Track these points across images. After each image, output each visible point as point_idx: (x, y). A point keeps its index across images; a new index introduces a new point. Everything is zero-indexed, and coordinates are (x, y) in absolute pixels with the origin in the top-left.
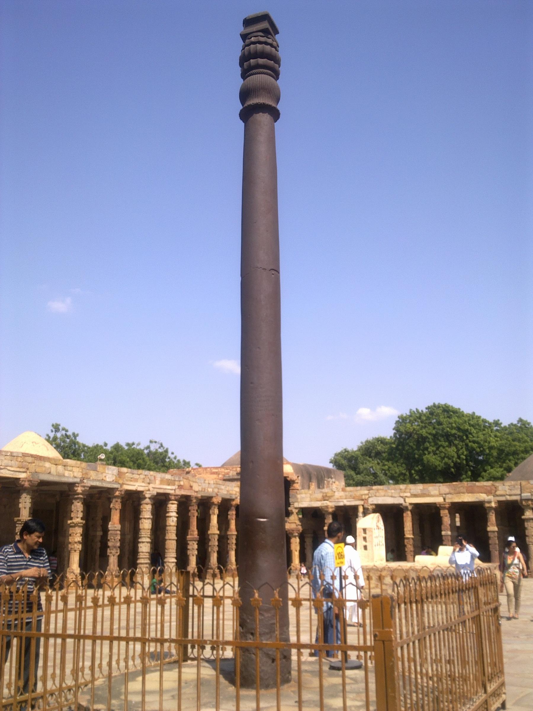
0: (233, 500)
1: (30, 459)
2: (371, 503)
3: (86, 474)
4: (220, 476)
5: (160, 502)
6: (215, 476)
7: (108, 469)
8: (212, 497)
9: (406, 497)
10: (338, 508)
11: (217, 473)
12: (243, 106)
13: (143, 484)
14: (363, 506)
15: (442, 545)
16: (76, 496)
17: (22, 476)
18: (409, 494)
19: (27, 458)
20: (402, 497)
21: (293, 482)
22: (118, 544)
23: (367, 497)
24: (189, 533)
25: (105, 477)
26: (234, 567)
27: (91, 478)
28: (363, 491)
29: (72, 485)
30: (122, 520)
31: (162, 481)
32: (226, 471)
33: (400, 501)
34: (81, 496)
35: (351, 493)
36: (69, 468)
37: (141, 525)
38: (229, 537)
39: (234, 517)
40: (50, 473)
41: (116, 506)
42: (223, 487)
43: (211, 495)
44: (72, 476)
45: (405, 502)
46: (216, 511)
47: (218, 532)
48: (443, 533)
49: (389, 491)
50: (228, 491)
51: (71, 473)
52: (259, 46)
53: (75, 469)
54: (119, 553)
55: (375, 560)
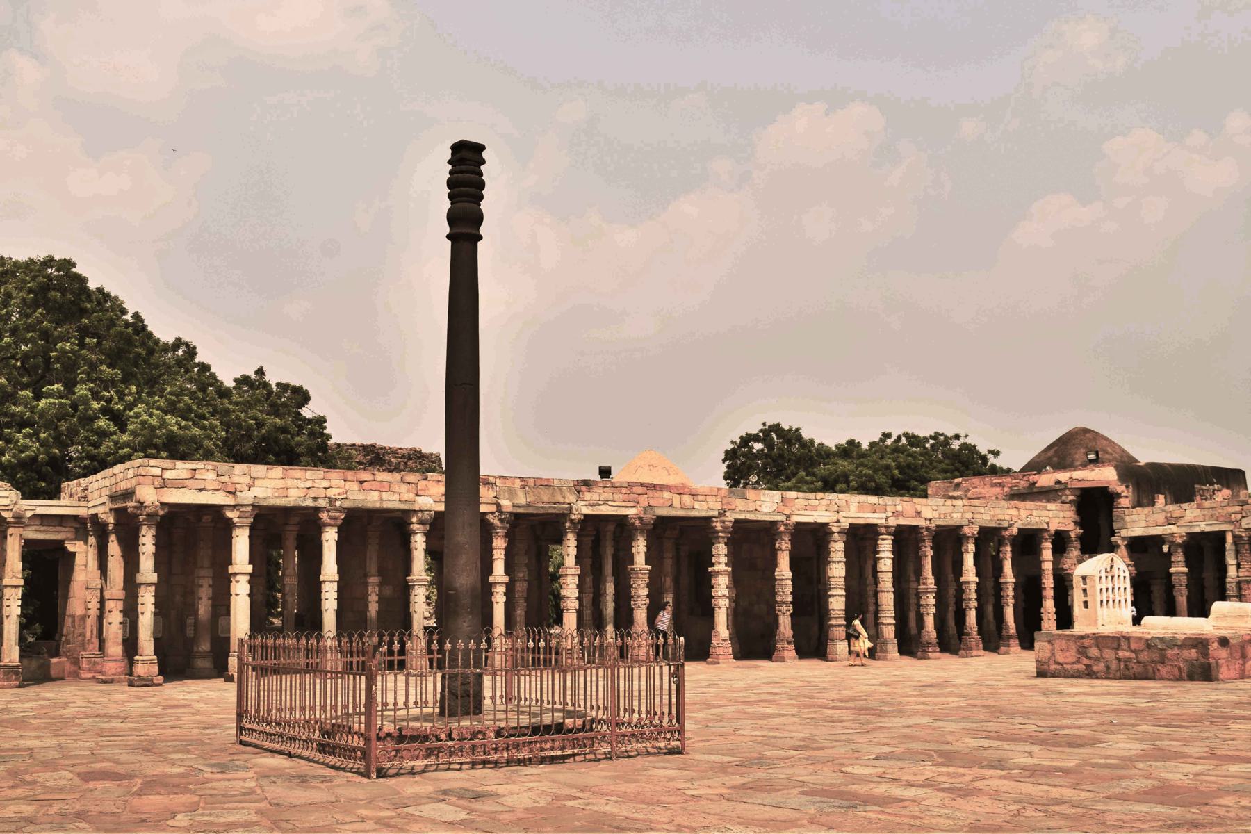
0: (1006, 529)
1: (640, 490)
5: (861, 539)
6: (998, 490)
8: (962, 526)
10: (1191, 536)
13: (827, 513)
15: (1223, 598)
17: (631, 512)
19: (635, 489)
21: (1119, 495)
22: (790, 598)
26: (1013, 631)
30: (793, 567)
31: (861, 507)
35: (1211, 512)
36: (700, 498)
39: (1009, 555)
40: (671, 506)
42: (982, 510)
46: (971, 547)
47: (977, 579)
50: (994, 516)
53: (709, 498)
55: (1100, 622)
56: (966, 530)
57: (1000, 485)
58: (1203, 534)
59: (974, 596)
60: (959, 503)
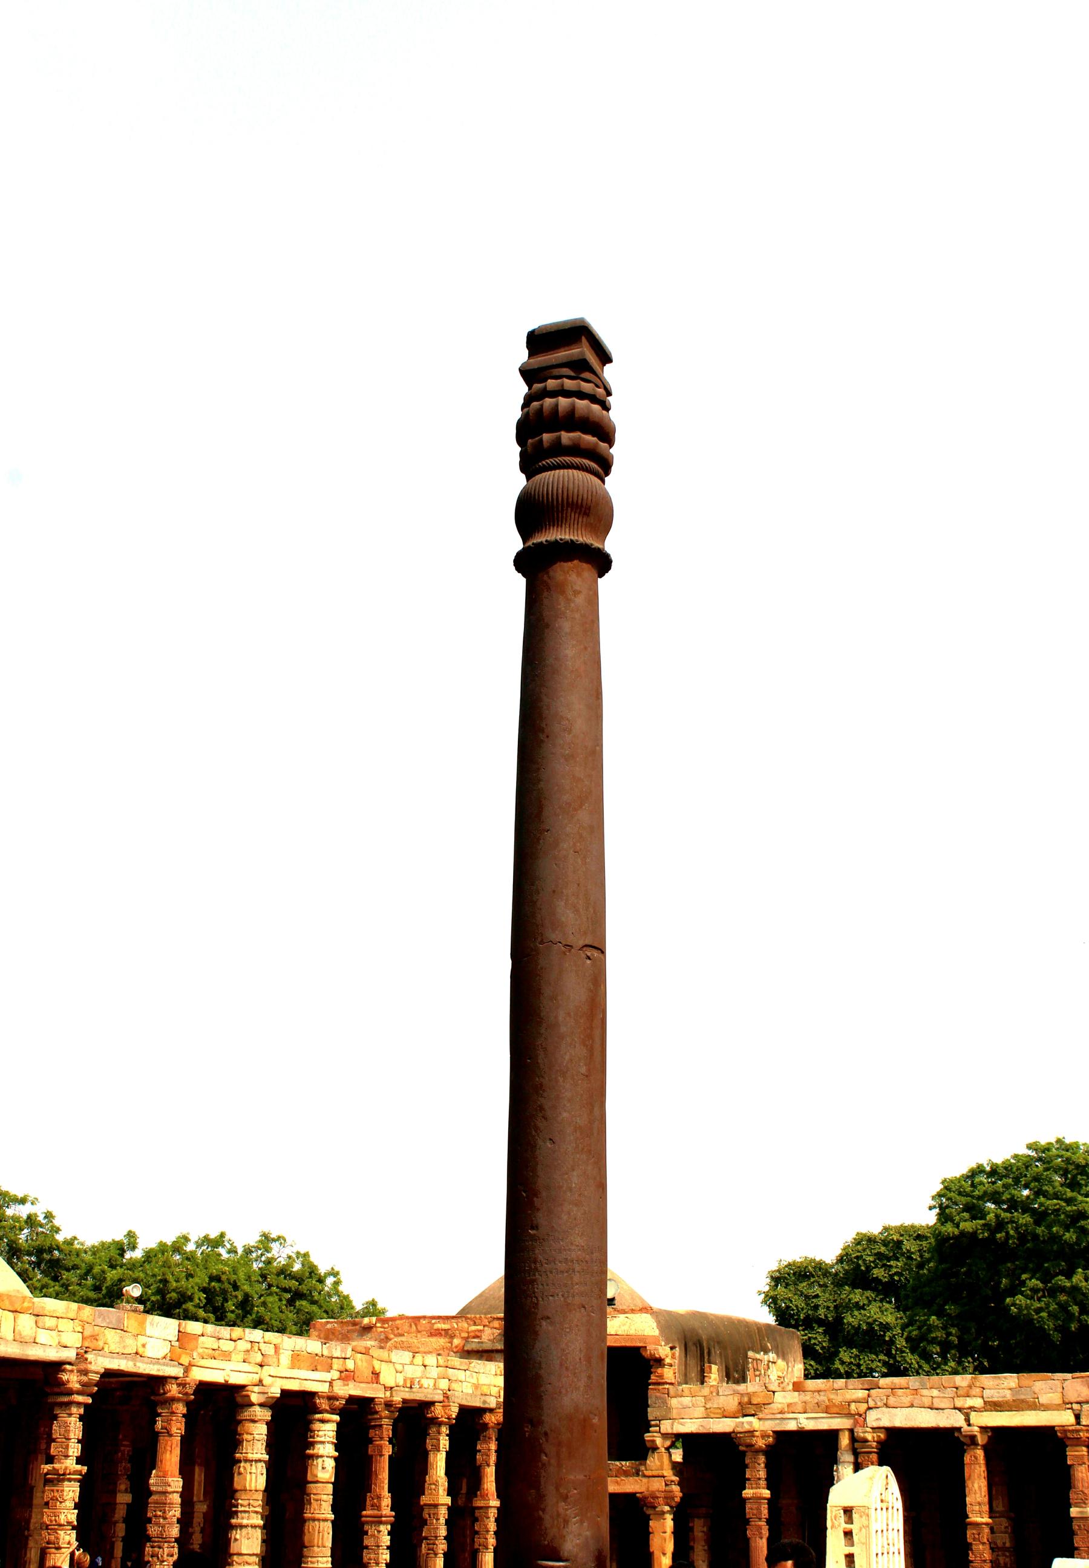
2: (875, 1425)
3: (94, 1337)
4: (456, 1341)
6: (442, 1341)
7: (152, 1324)
8: (433, 1403)
9: (971, 1408)
10: (782, 1437)
11: (446, 1333)
12: (524, 543)
13: (246, 1367)
14: (851, 1431)
16: (66, 1399)
18: (978, 1402)
20: (960, 1409)
21: (659, 1362)
22: (175, 1531)
23: (863, 1407)
24: (368, 1503)
25: (144, 1346)
27: (106, 1349)
28: (851, 1391)
29: (56, 1366)
31: (297, 1359)
32: (473, 1328)
33: (956, 1420)
34: (80, 1398)
36: (50, 1322)
37: (236, 1478)
38: (477, 1513)
39: (493, 1458)
41: (174, 1426)
42: (461, 1375)
43: (429, 1398)
44: (55, 1343)
45: (969, 1425)
46: (444, 1442)
48: (1074, 1511)
49: (925, 1392)
50: (476, 1386)
51: (54, 1333)
52: (563, 402)
53: (64, 1325)
54: (176, 1557)
56: (438, 1411)
57: (446, 1333)
58: (801, 1435)
59: (443, 1532)
60: (431, 1360)
